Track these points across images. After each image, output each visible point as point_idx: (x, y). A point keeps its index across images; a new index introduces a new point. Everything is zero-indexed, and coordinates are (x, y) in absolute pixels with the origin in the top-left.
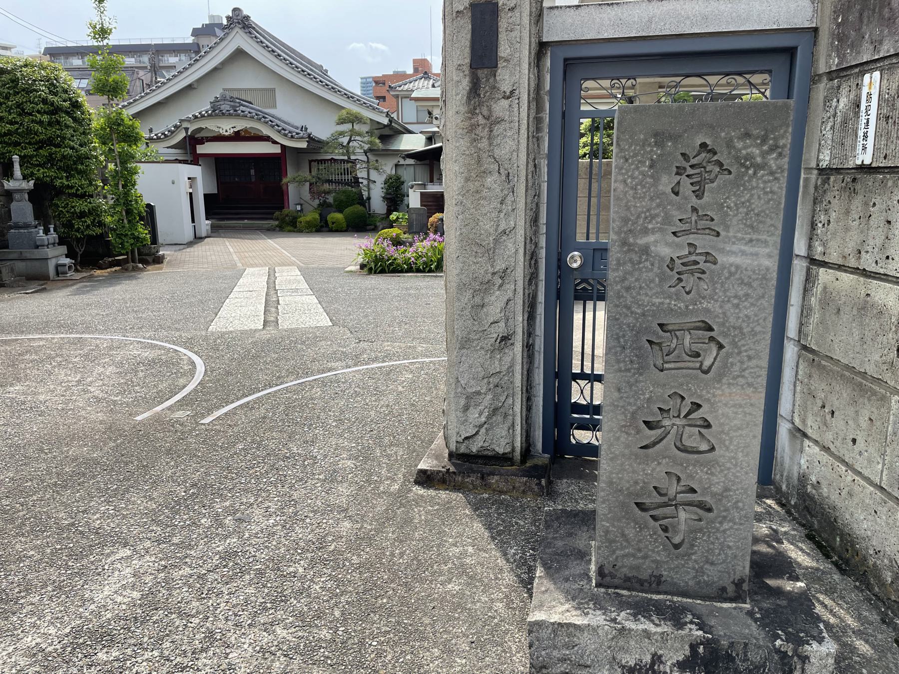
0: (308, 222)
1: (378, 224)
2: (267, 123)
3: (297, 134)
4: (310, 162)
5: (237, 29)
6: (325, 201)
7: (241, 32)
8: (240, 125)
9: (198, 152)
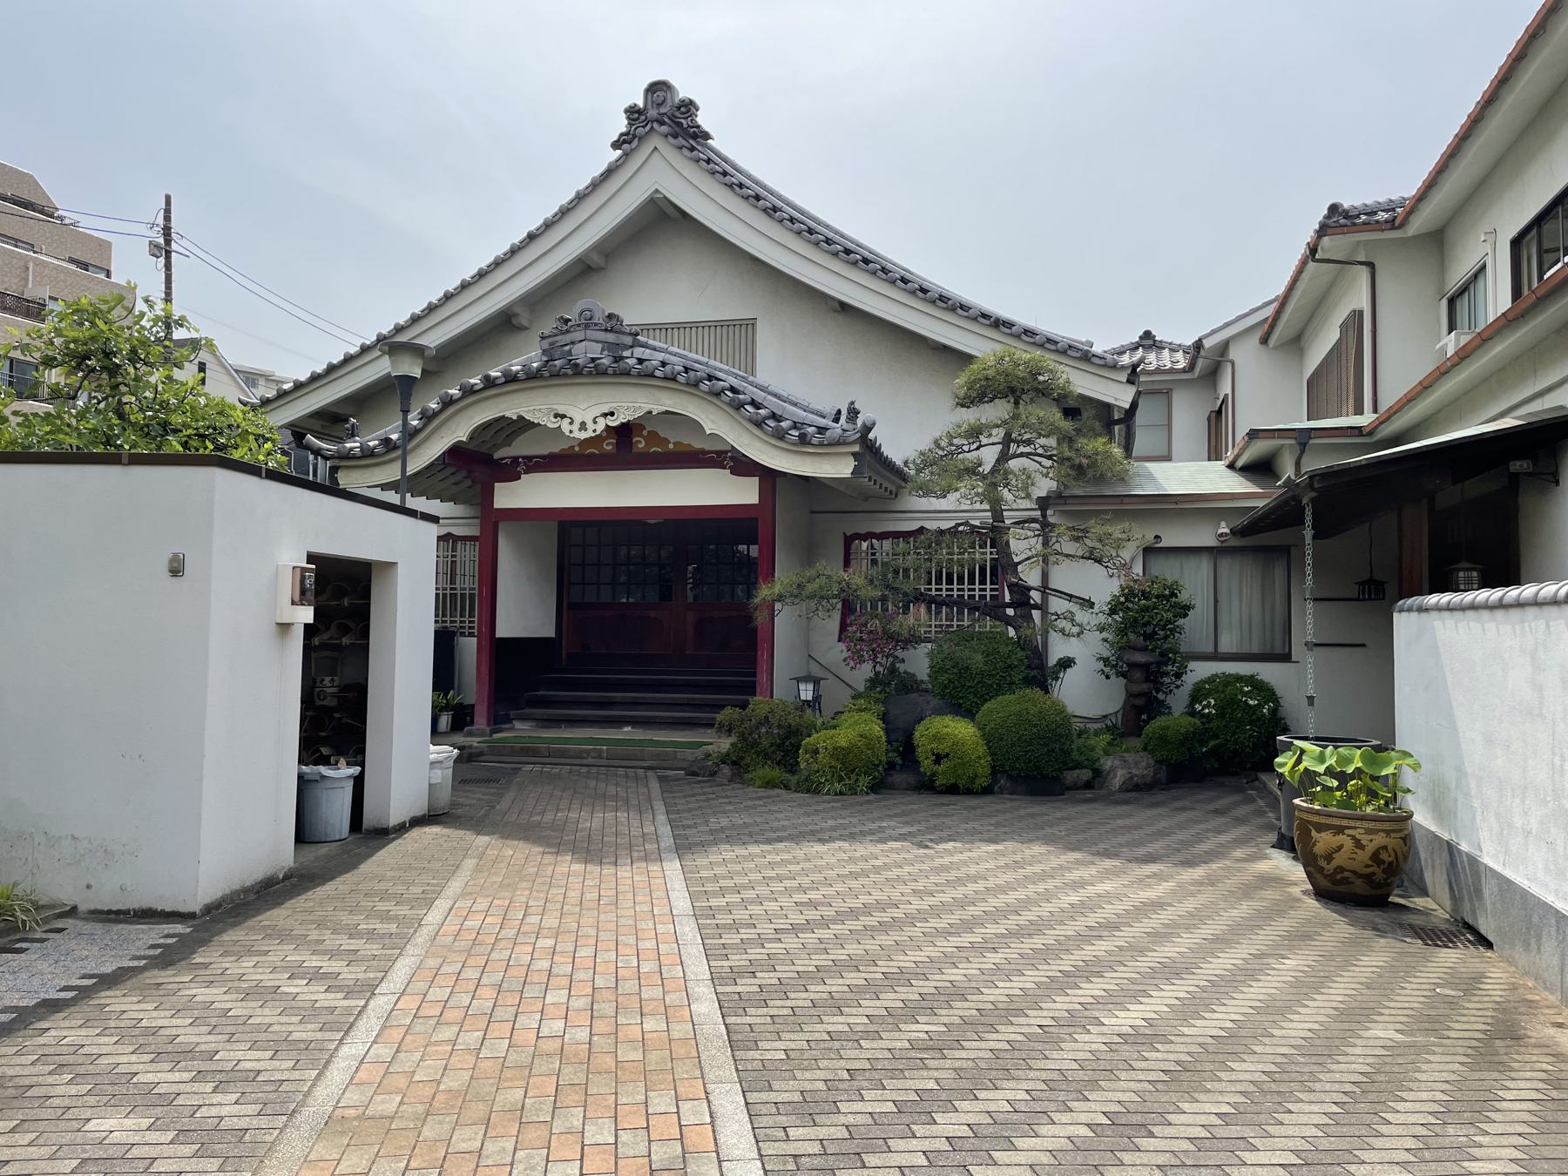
0: (839, 754)
1: (1107, 763)
2: (718, 394)
3: (822, 430)
4: (849, 541)
5: (655, 141)
6: (893, 670)
7: (665, 148)
8: (630, 404)
9: (496, 506)
